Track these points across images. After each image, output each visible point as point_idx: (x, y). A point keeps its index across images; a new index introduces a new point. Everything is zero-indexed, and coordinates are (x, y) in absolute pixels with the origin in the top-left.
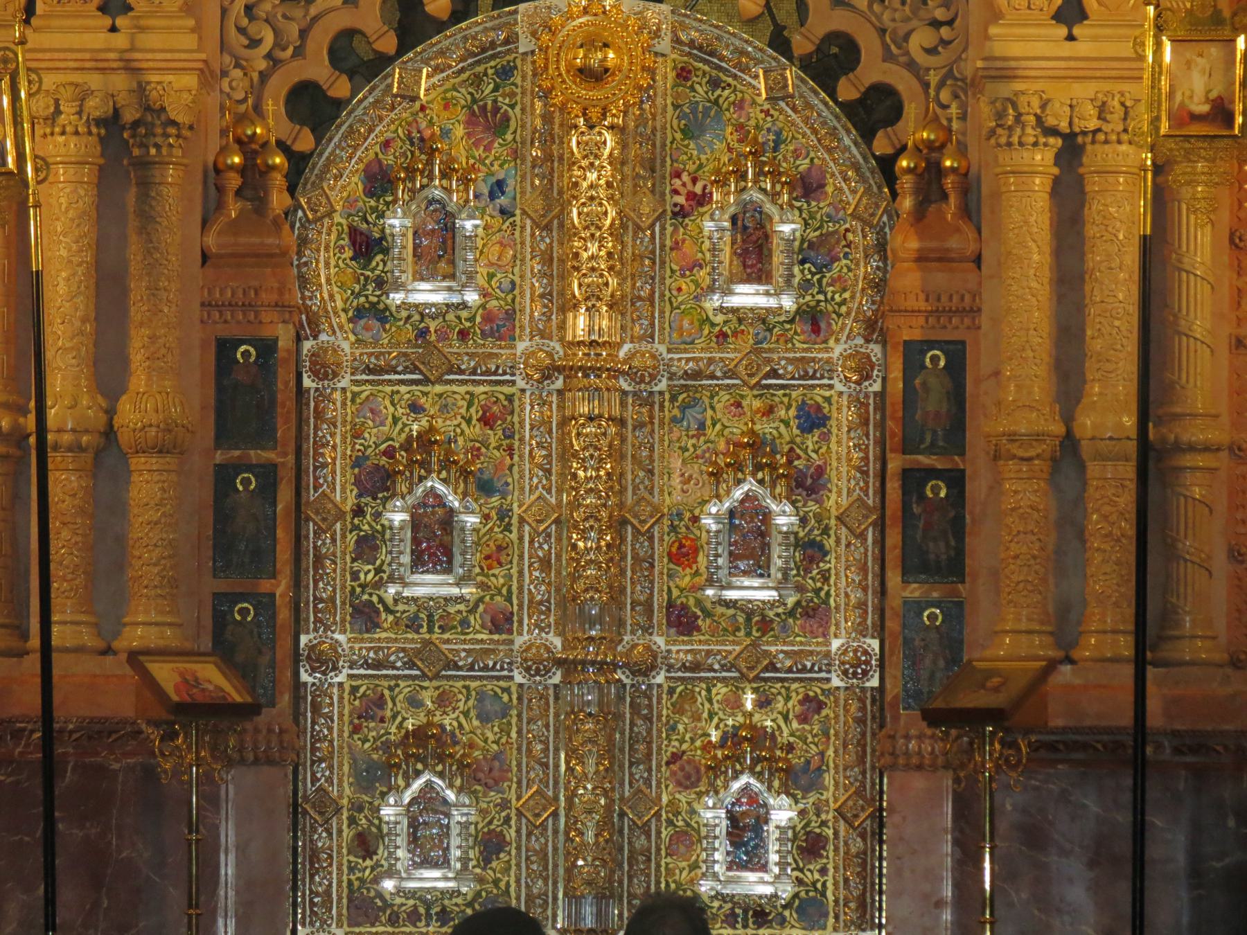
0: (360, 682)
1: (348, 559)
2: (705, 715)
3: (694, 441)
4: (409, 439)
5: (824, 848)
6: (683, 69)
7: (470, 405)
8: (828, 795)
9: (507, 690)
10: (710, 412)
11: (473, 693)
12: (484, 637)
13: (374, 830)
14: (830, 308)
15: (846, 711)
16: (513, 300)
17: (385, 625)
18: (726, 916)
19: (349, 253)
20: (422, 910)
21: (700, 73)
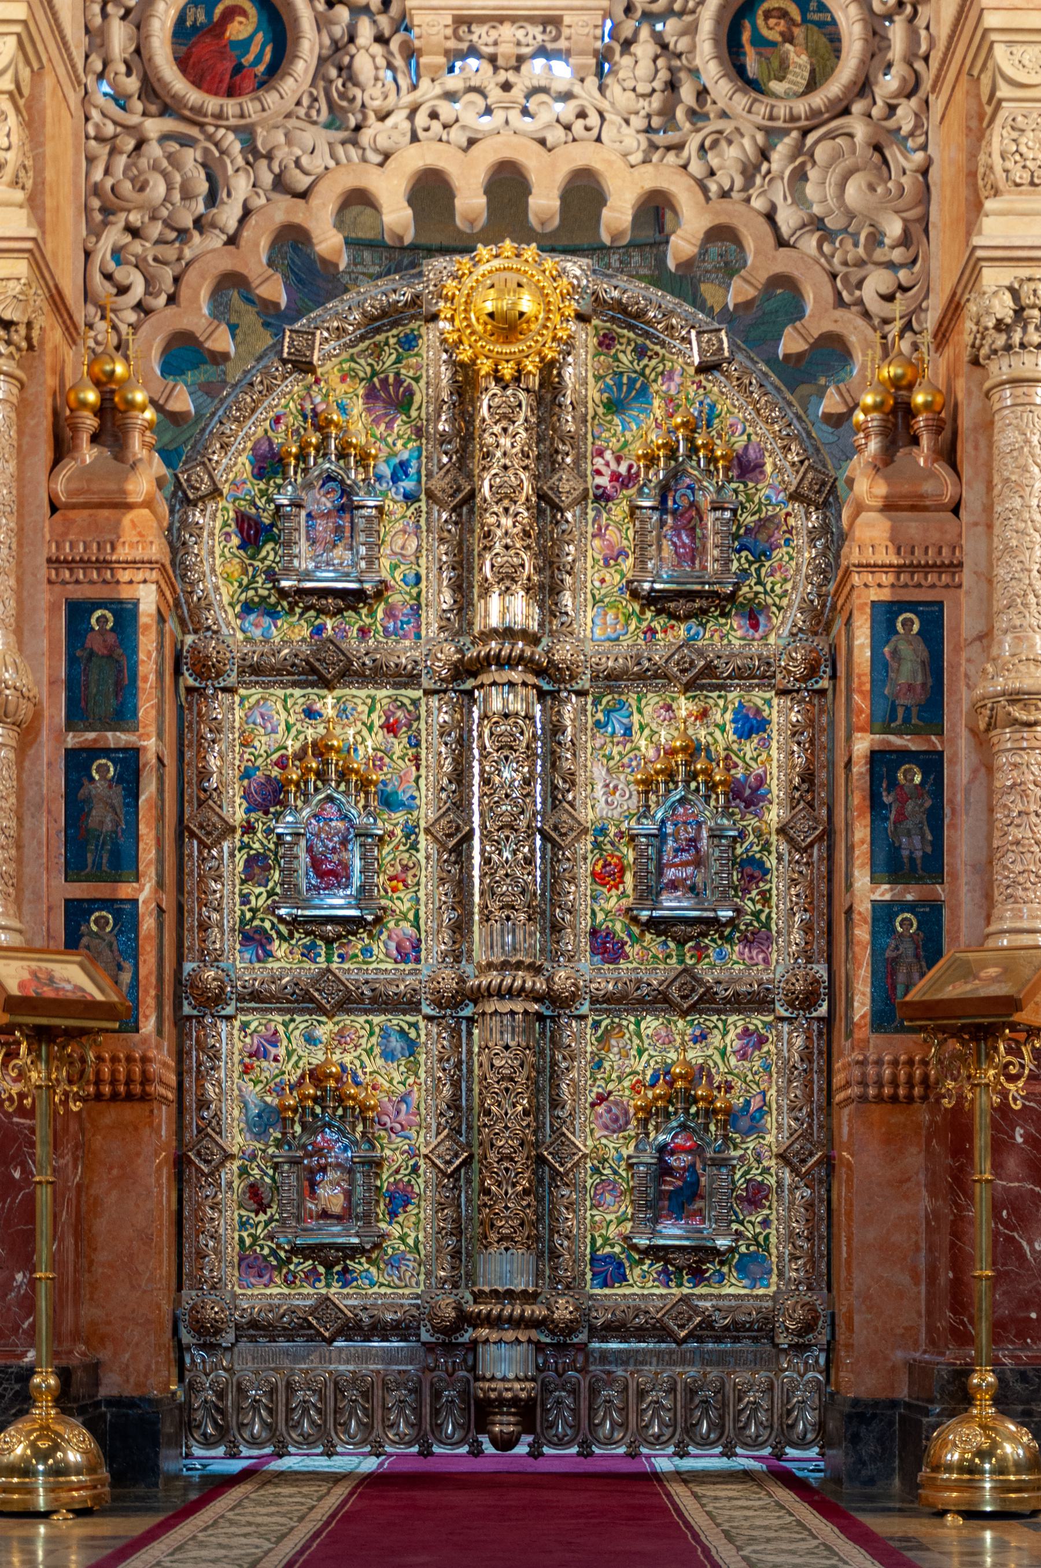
0: (250, 1018)
1: (237, 881)
2: (633, 1052)
3: (620, 748)
4: (304, 749)
5: (766, 1197)
6: (605, 336)
7: (372, 710)
8: (770, 1138)
9: (414, 1025)
10: (636, 717)
11: (377, 1029)
12: (390, 966)
13: (267, 1180)
14: (770, 601)
15: (790, 1044)
16: (419, 594)
17: (280, 954)
18: (659, 1273)
19: (235, 541)
20: (321, 1269)
21: (624, 340)
